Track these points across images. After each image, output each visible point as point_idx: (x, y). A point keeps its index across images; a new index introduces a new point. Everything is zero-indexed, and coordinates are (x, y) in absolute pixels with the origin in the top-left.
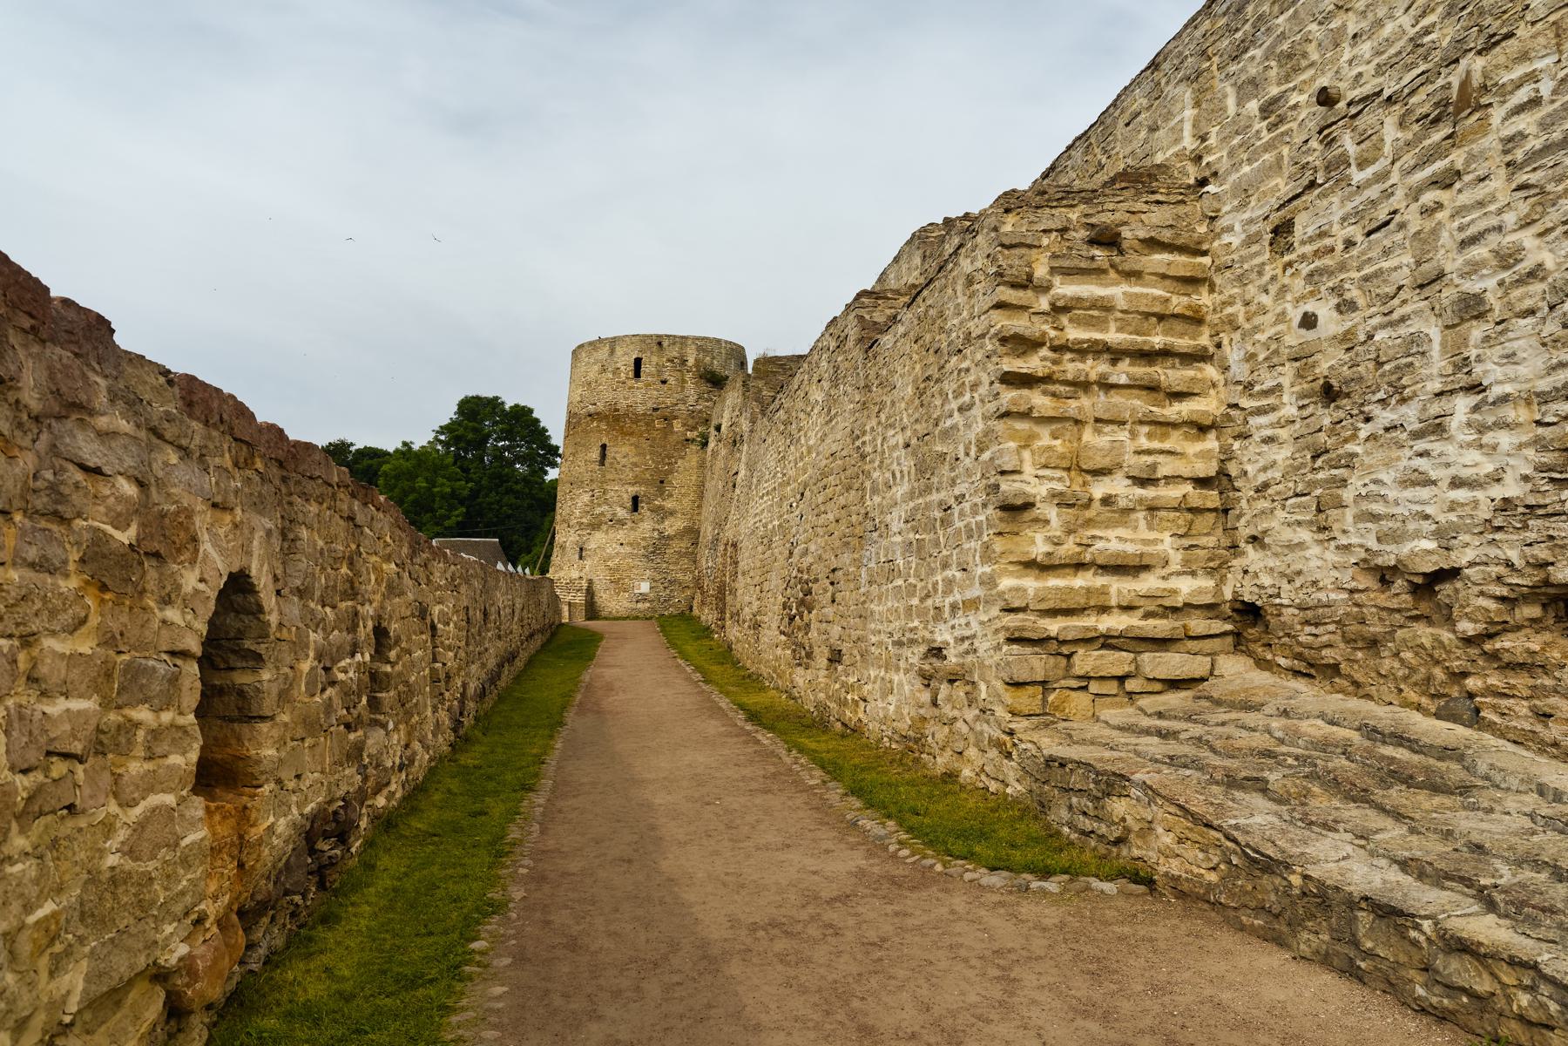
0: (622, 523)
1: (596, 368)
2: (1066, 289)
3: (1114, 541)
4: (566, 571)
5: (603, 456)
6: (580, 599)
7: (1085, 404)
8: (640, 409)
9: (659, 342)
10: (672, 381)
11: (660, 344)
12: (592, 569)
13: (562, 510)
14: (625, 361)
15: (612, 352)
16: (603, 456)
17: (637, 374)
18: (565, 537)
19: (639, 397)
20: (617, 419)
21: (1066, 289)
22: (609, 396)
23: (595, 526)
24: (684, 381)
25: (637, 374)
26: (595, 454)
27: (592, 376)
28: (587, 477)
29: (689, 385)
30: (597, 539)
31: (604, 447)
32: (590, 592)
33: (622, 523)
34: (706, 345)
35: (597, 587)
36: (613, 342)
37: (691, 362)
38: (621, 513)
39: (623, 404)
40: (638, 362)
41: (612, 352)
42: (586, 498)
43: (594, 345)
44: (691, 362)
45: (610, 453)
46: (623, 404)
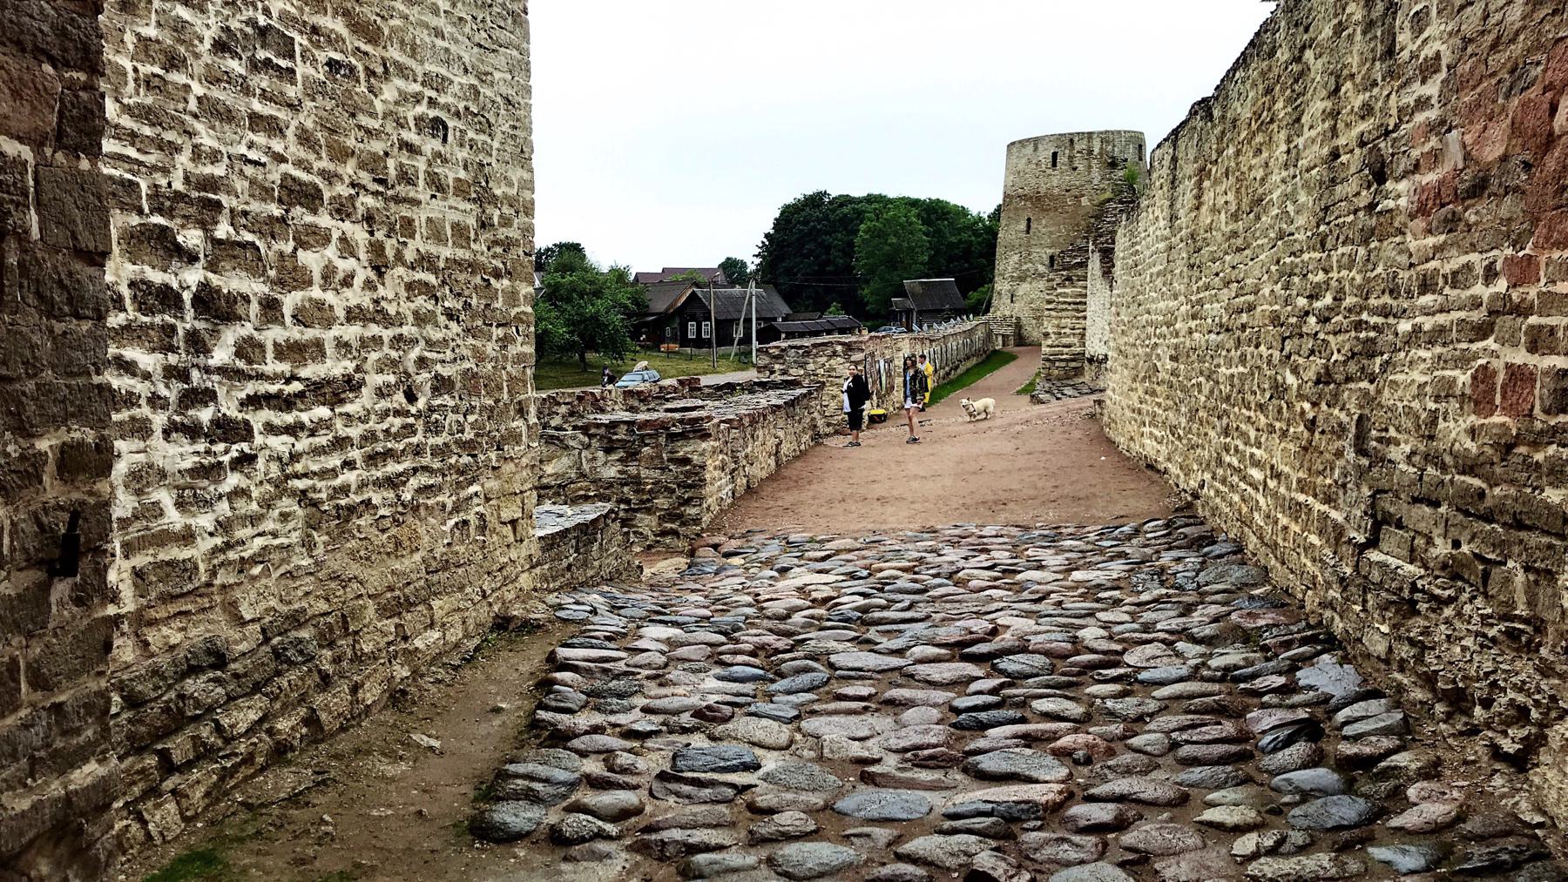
0: (1042, 276)
1: (1024, 161)
2: (1060, 290)
3: (1065, 341)
4: (1002, 308)
5: (1029, 227)
6: (1010, 331)
7: (1064, 314)
8: (1056, 191)
9: (1070, 140)
10: (1081, 167)
11: (1072, 141)
12: (1020, 310)
13: (1000, 266)
14: (1045, 155)
15: (1036, 149)
16: (1029, 227)
17: (1054, 165)
18: (1002, 286)
19: (1057, 181)
20: (1038, 199)
21: (1060, 290)
22: (1033, 181)
23: (1022, 279)
24: (1090, 167)
25: (1054, 165)
26: (1023, 226)
27: (1020, 167)
28: (1017, 242)
29: (1095, 169)
30: (1024, 288)
31: (1029, 220)
32: (1018, 326)
33: (1042, 276)
34: (1107, 137)
35: (1024, 321)
36: (1036, 142)
37: (1096, 151)
38: (1041, 269)
39: (1043, 190)
40: (1055, 155)
41: (1036, 149)
42: (1016, 258)
43: (1022, 143)
44: (1096, 151)
45: (1033, 225)
46: (1043, 190)
